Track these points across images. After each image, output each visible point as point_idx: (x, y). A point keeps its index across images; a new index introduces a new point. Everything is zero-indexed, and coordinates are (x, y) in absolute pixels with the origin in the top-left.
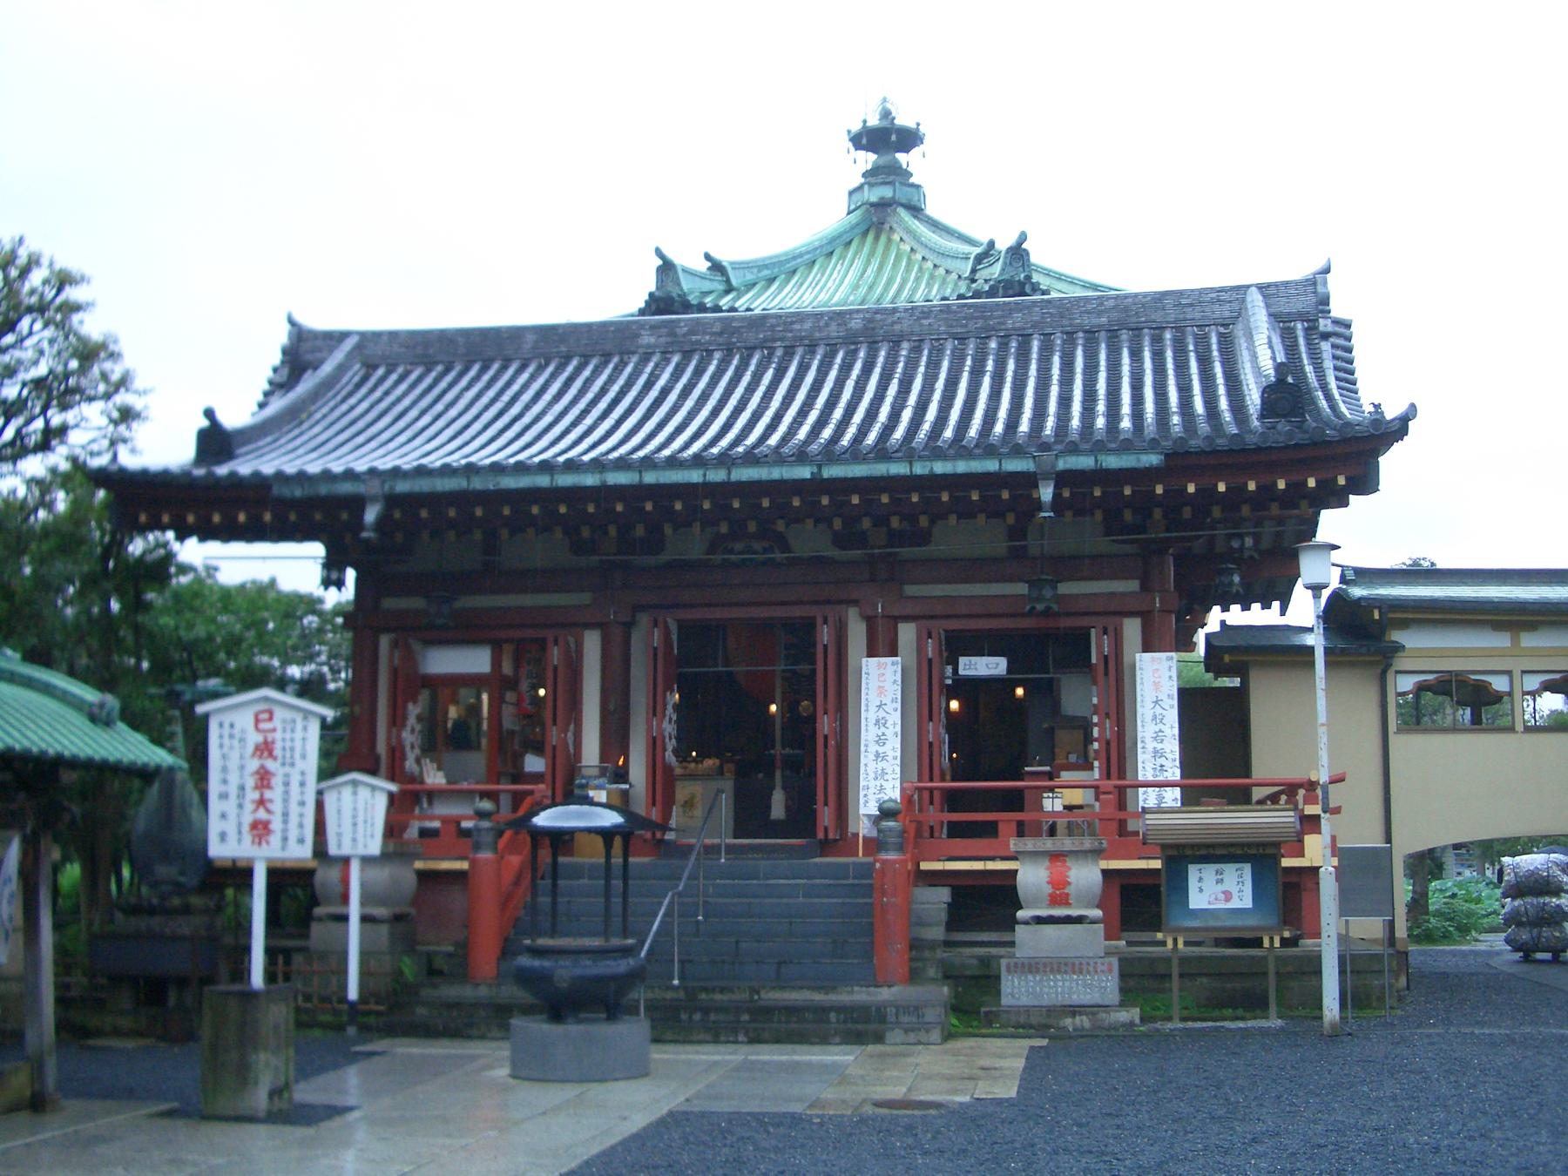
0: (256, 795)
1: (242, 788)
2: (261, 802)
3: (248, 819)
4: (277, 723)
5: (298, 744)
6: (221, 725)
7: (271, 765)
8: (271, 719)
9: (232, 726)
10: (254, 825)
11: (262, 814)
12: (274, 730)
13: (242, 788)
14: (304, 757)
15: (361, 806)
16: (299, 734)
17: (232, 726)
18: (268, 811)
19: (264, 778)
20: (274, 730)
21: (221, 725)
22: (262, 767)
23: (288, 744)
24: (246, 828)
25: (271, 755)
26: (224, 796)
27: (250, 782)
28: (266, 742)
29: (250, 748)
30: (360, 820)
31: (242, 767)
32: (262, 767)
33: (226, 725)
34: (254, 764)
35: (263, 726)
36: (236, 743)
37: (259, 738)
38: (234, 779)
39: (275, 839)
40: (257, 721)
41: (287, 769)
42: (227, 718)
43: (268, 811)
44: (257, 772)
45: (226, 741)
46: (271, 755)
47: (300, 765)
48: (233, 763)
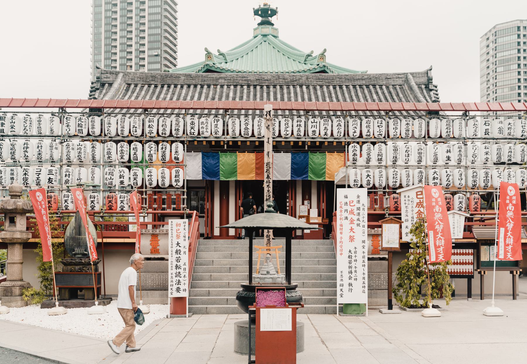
1: (413, 218)
6: (405, 196)
7: (422, 210)
9: (409, 197)
13: (413, 218)
15: (456, 222)
17: (409, 197)
21: (405, 196)
22: (419, 210)
25: (422, 206)
26: (407, 220)
28: (420, 202)
29: (415, 204)
30: (456, 227)
31: (413, 211)
32: (419, 210)
33: (407, 197)
34: (416, 210)
35: (418, 197)
36: (410, 202)
37: (418, 201)
38: (410, 215)
40: (417, 195)
42: (407, 194)
44: (417, 212)
45: (407, 202)
48: (410, 209)
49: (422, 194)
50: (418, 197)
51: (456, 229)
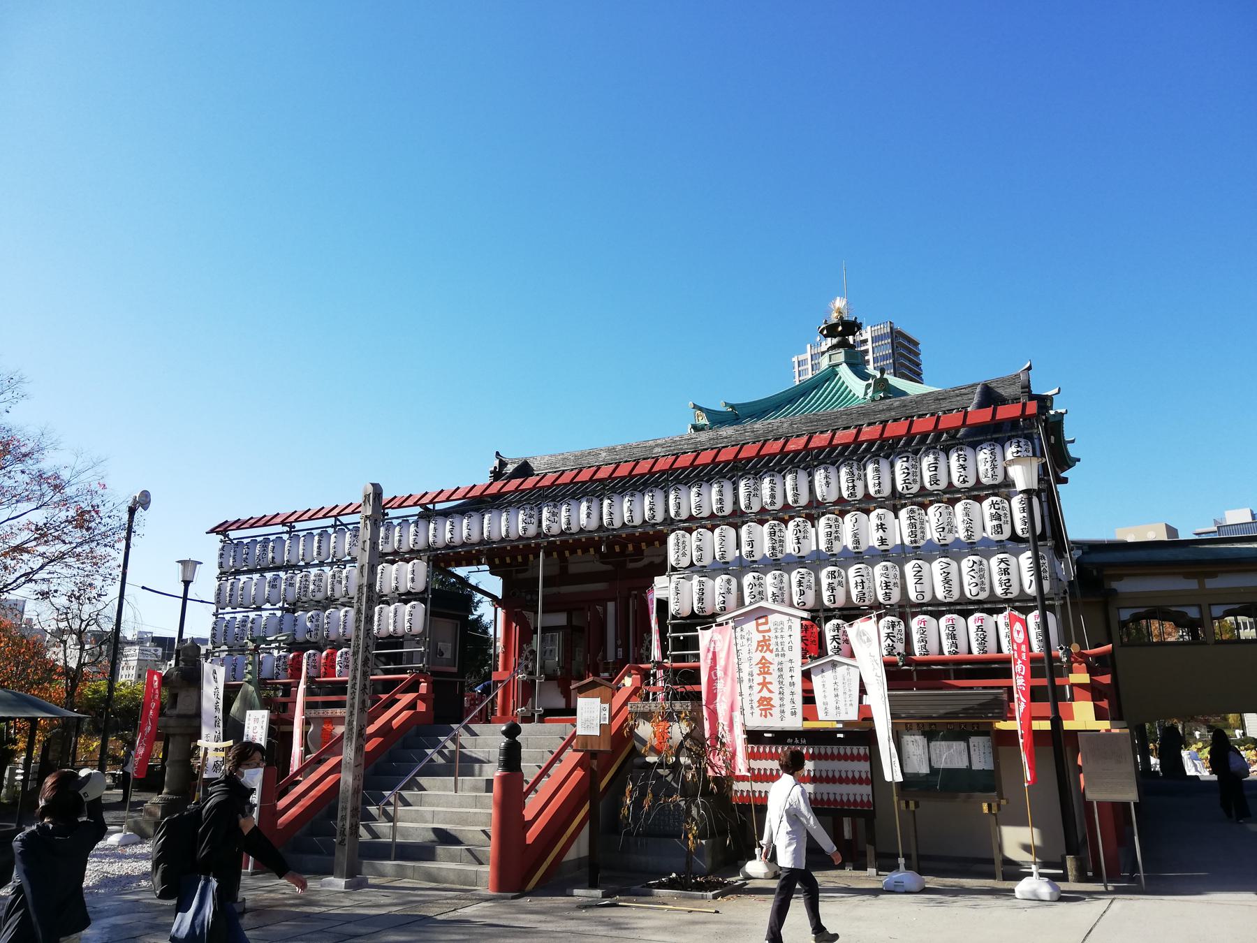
0: (760, 679)
2: (764, 684)
3: (756, 698)
4: (770, 625)
5: (787, 639)
7: (768, 656)
8: (766, 623)
10: (762, 700)
11: (765, 693)
12: (769, 631)
14: (791, 649)
16: (786, 634)
18: (770, 691)
19: (764, 666)
20: (769, 631)
22: (763, 658)
23: (779, 640)
24: (755, 704)
25: (768, 649)
27: (756, 670)
28: (764, 640)
29: (755, 644)
30: (840, 693)
32: (763, 658)
35: (761, 628)
36: (745, 641)
39: (776, 711)
41: (780, 659)
43: (770, 691)
45: (739, 641)
46: (768, 649)
47: (789, 655)
49: (766, 623)
50: (761, 628)
51: (841, 697)
